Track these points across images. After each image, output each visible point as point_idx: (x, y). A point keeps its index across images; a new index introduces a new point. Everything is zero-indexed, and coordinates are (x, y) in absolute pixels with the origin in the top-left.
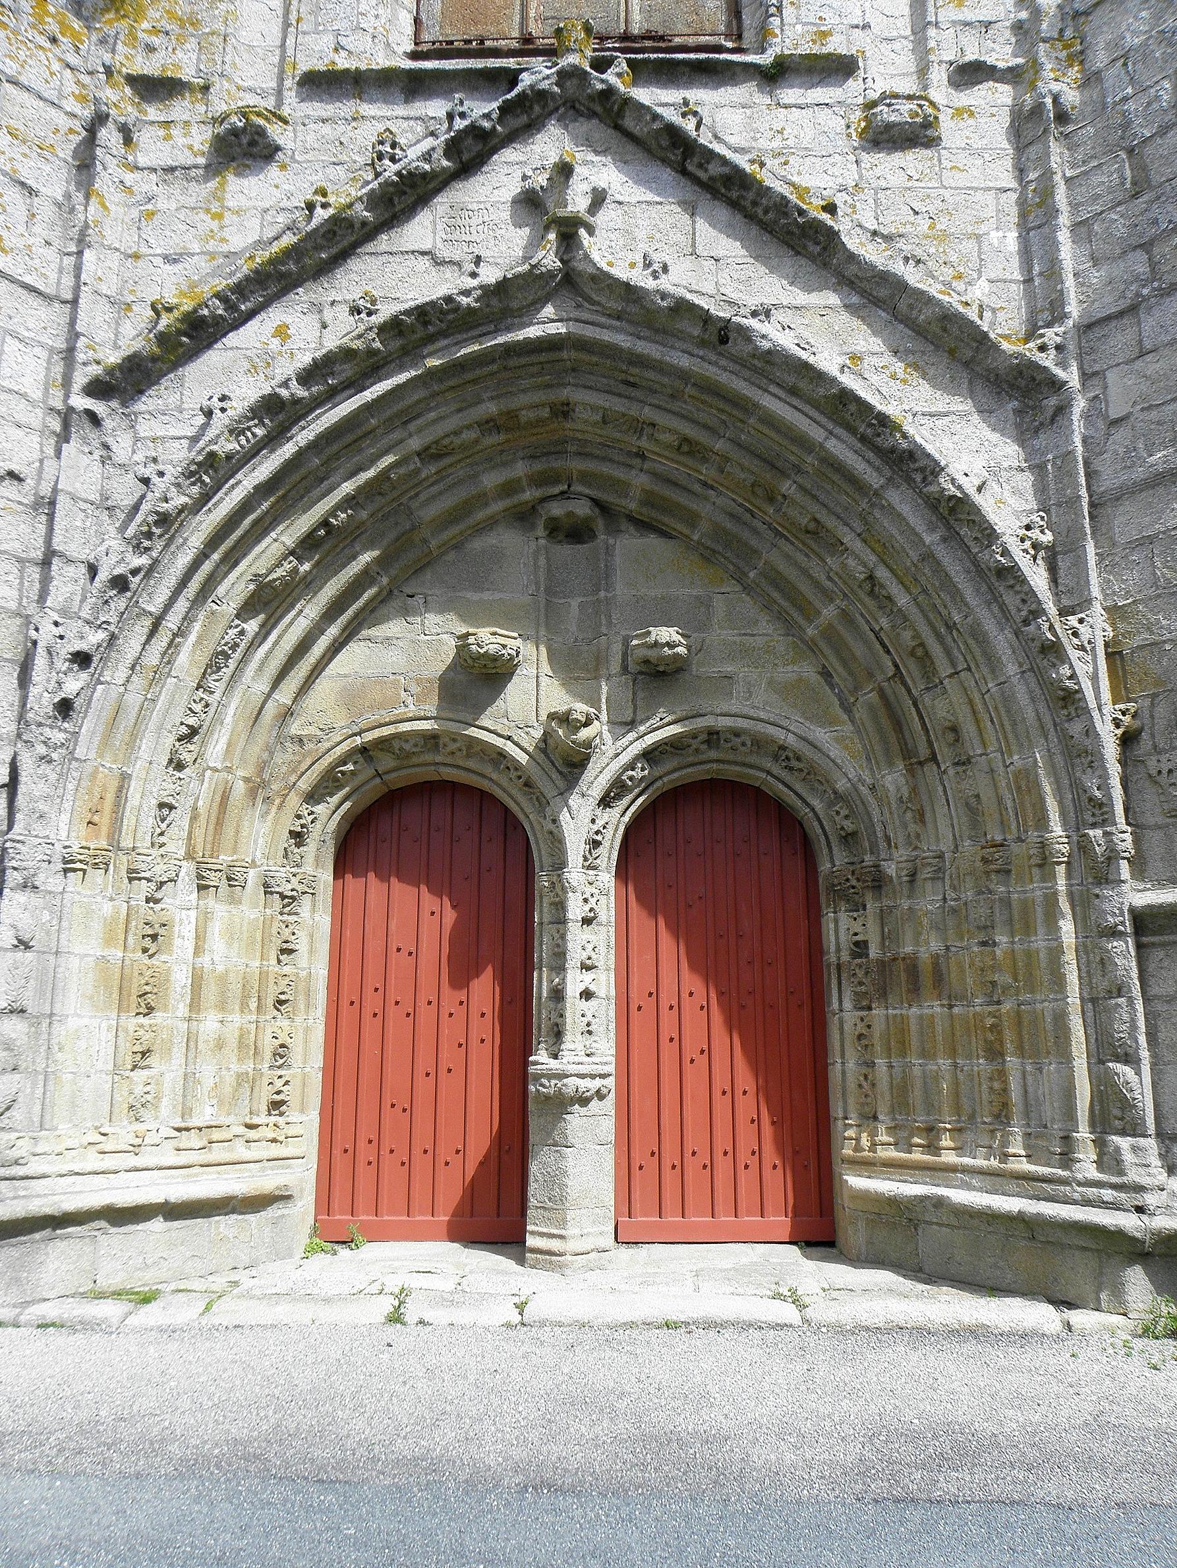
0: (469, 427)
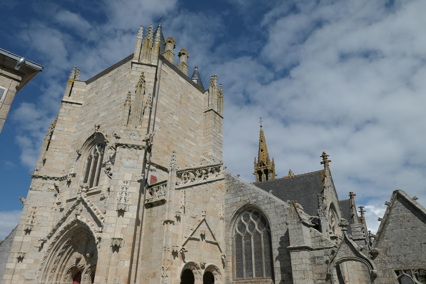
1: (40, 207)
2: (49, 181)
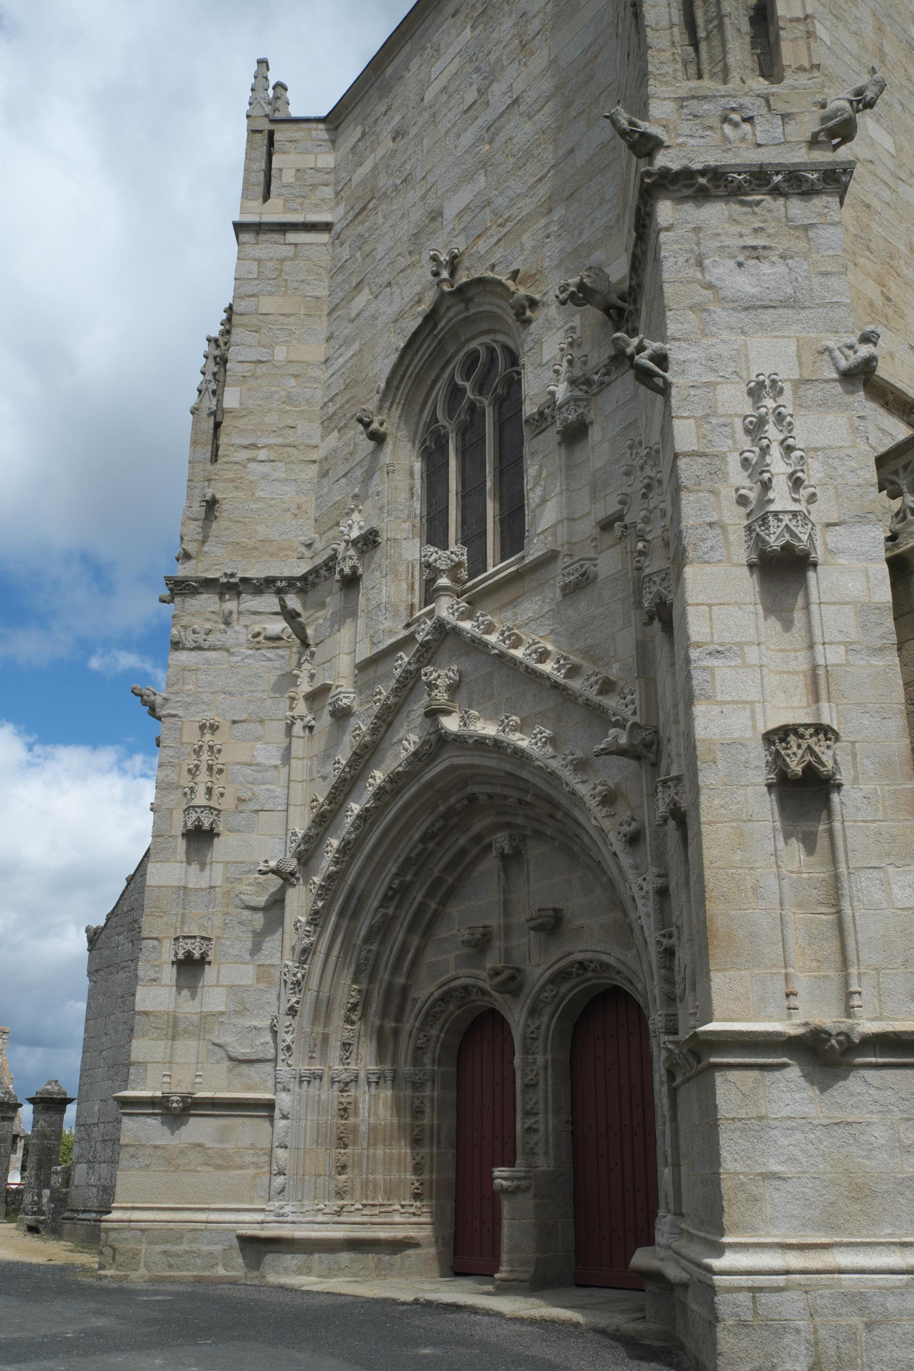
0: (437, 820)
1: (234, 722)
2: (250, 602)
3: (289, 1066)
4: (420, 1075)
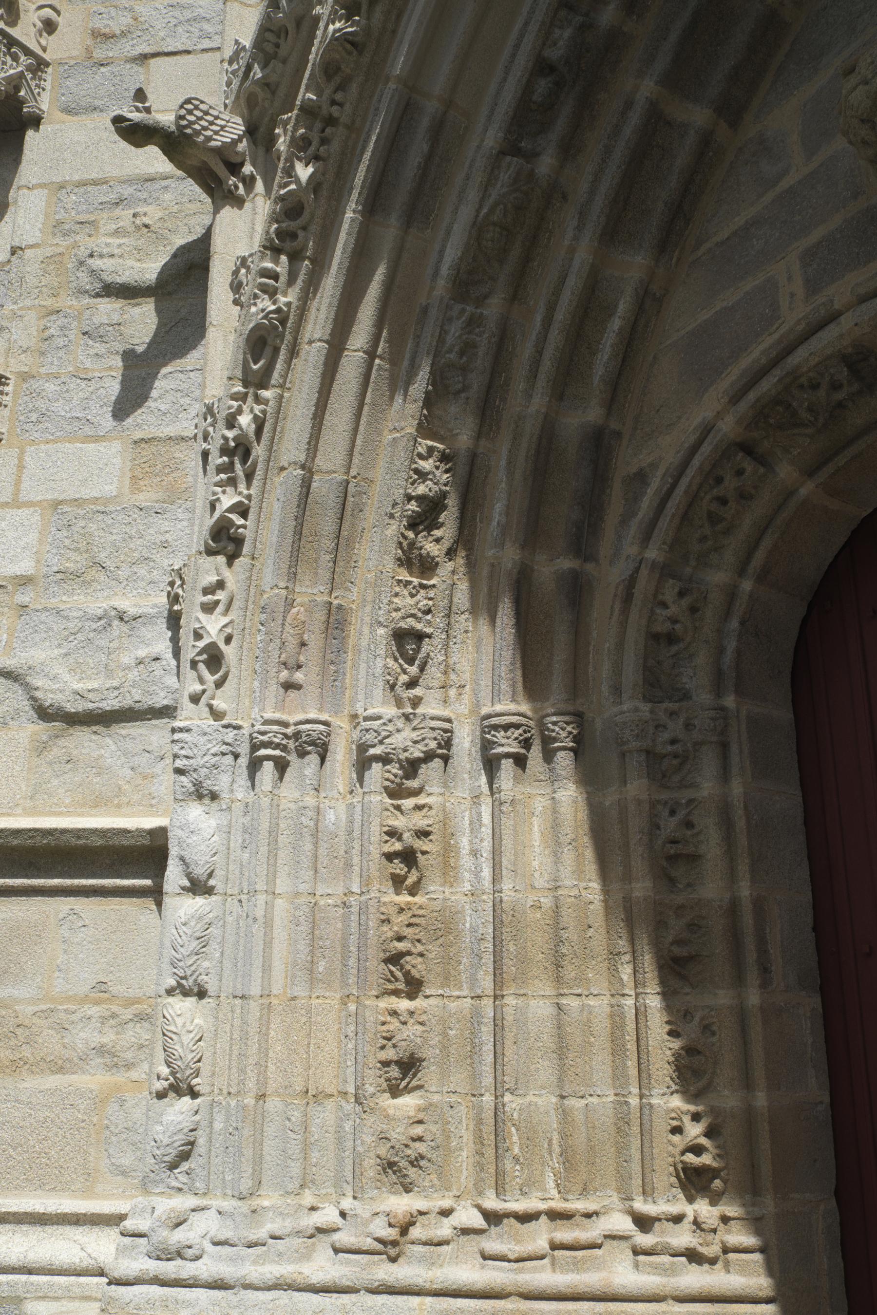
3: (217, 715)
4: (675, 728)
